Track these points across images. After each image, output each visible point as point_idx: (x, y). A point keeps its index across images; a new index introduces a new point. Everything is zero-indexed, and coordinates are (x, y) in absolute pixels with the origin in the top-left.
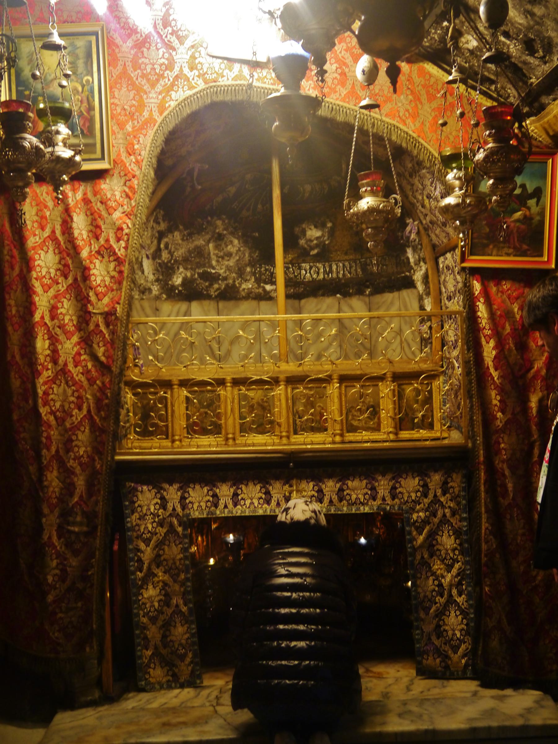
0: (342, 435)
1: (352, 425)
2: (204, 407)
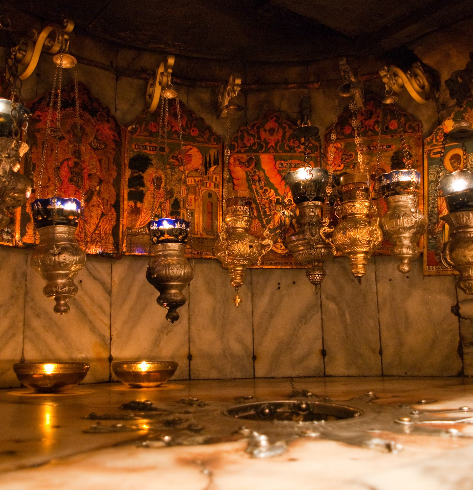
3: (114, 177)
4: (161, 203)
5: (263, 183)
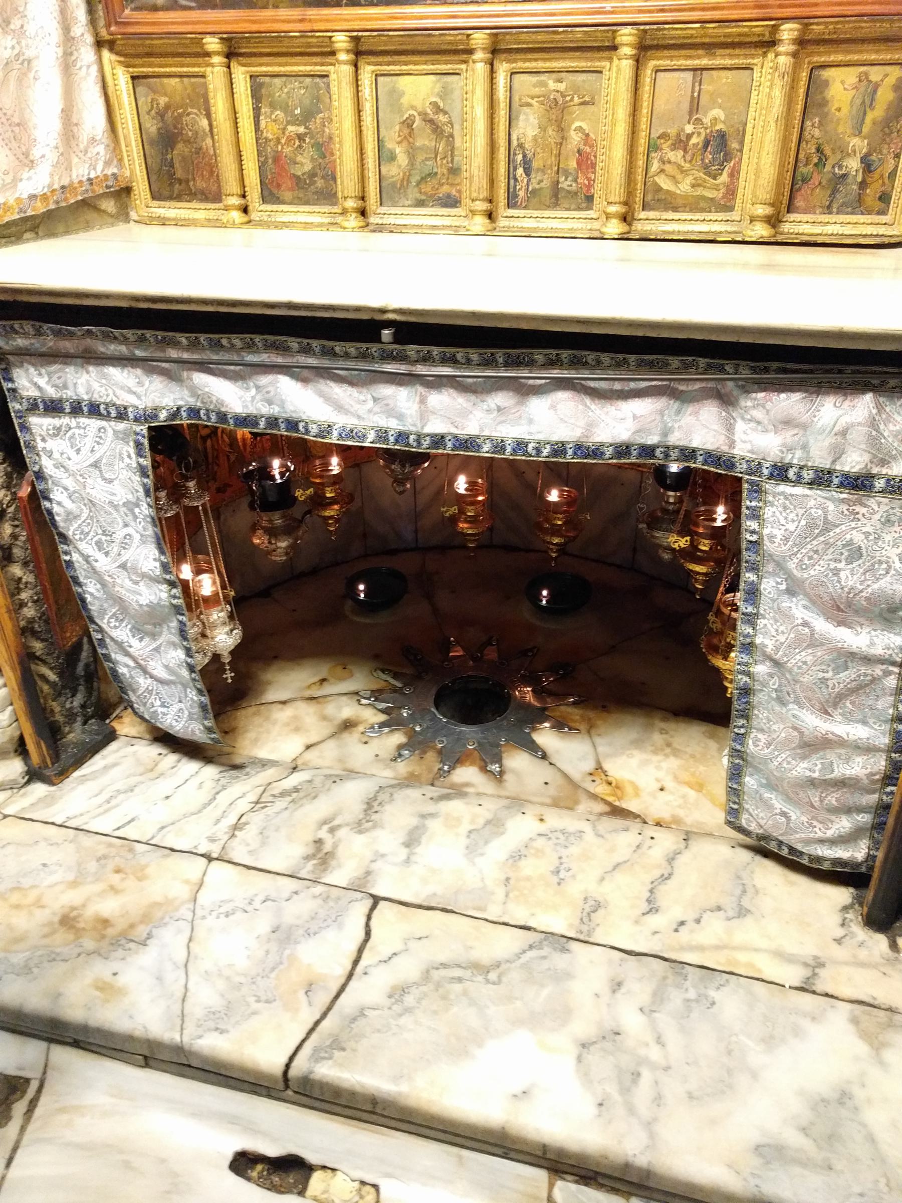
0: (625, 218)
1: (659, 189)
2: (296, 122)
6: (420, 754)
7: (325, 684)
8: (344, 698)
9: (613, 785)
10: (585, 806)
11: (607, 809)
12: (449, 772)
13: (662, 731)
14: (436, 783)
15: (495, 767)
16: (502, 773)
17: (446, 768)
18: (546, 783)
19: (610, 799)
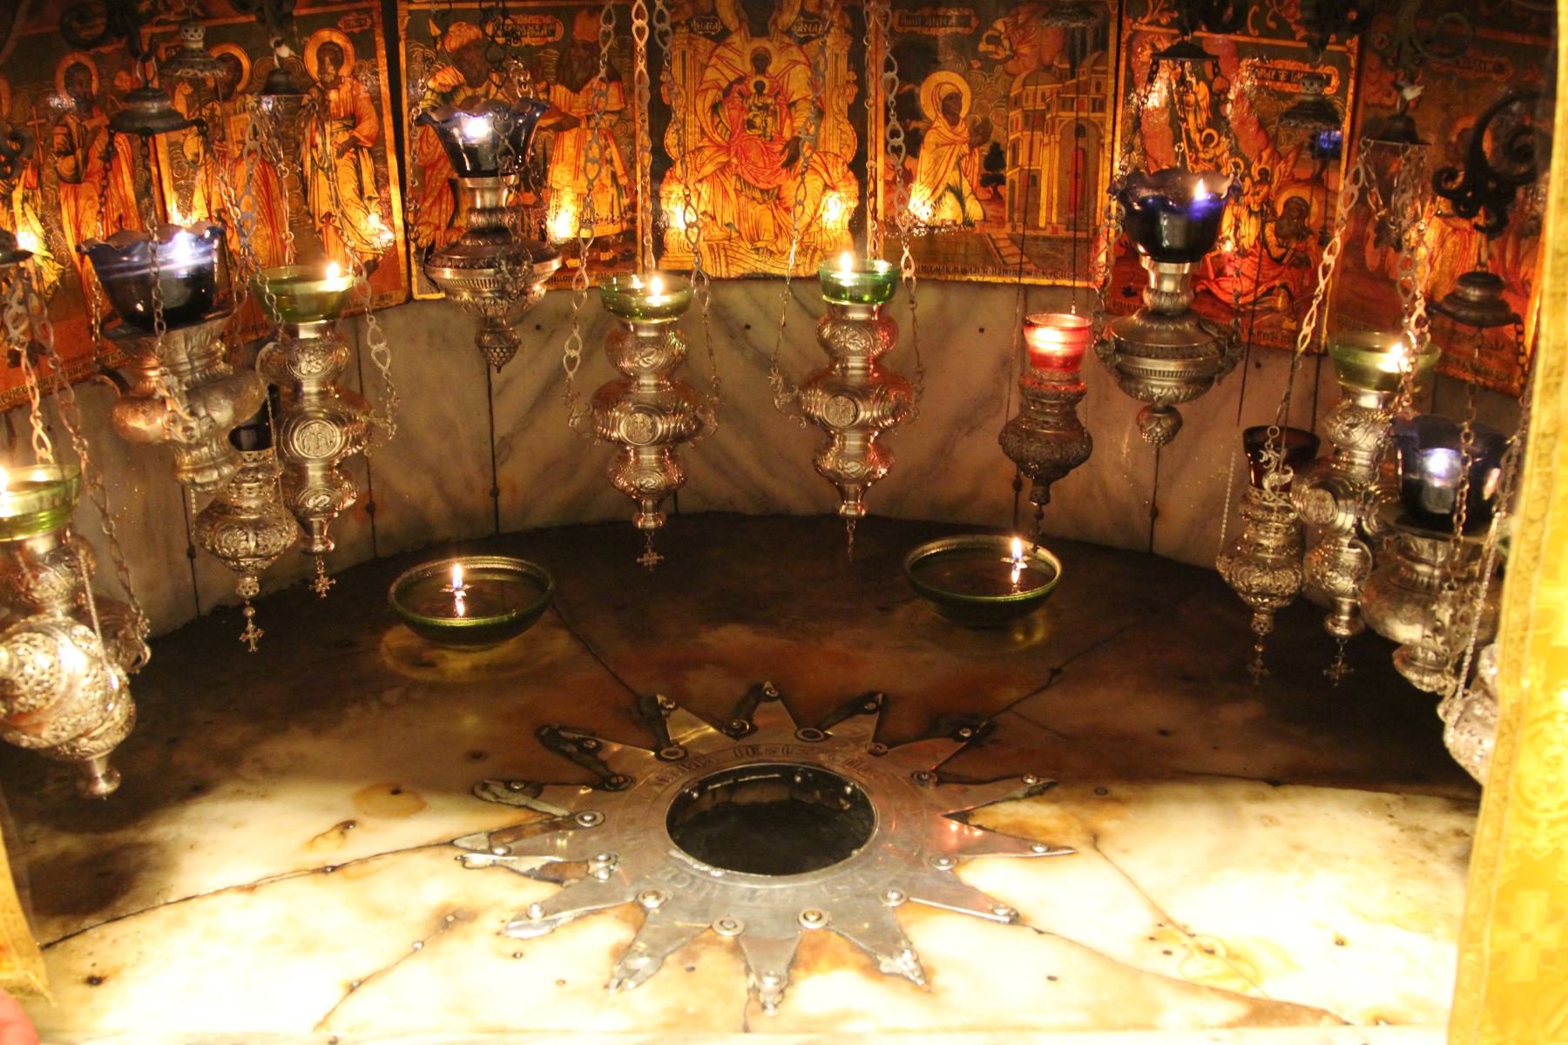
3: (851, 100)
4: (960, 159)
5: (1204, 116)
6: (681, 962)
7: (352, 831)
8: (420, 859)
9: (1221, 951)
10: (1177, 1010)
11: (1239, 1010)
12: (782, 991)
13: (1270, 821)
14: (753, 1023)
15: (903, 963)
16: (925, 973)
17: (769, 983)
18: (1051, 978)
19: (1234, 985)
